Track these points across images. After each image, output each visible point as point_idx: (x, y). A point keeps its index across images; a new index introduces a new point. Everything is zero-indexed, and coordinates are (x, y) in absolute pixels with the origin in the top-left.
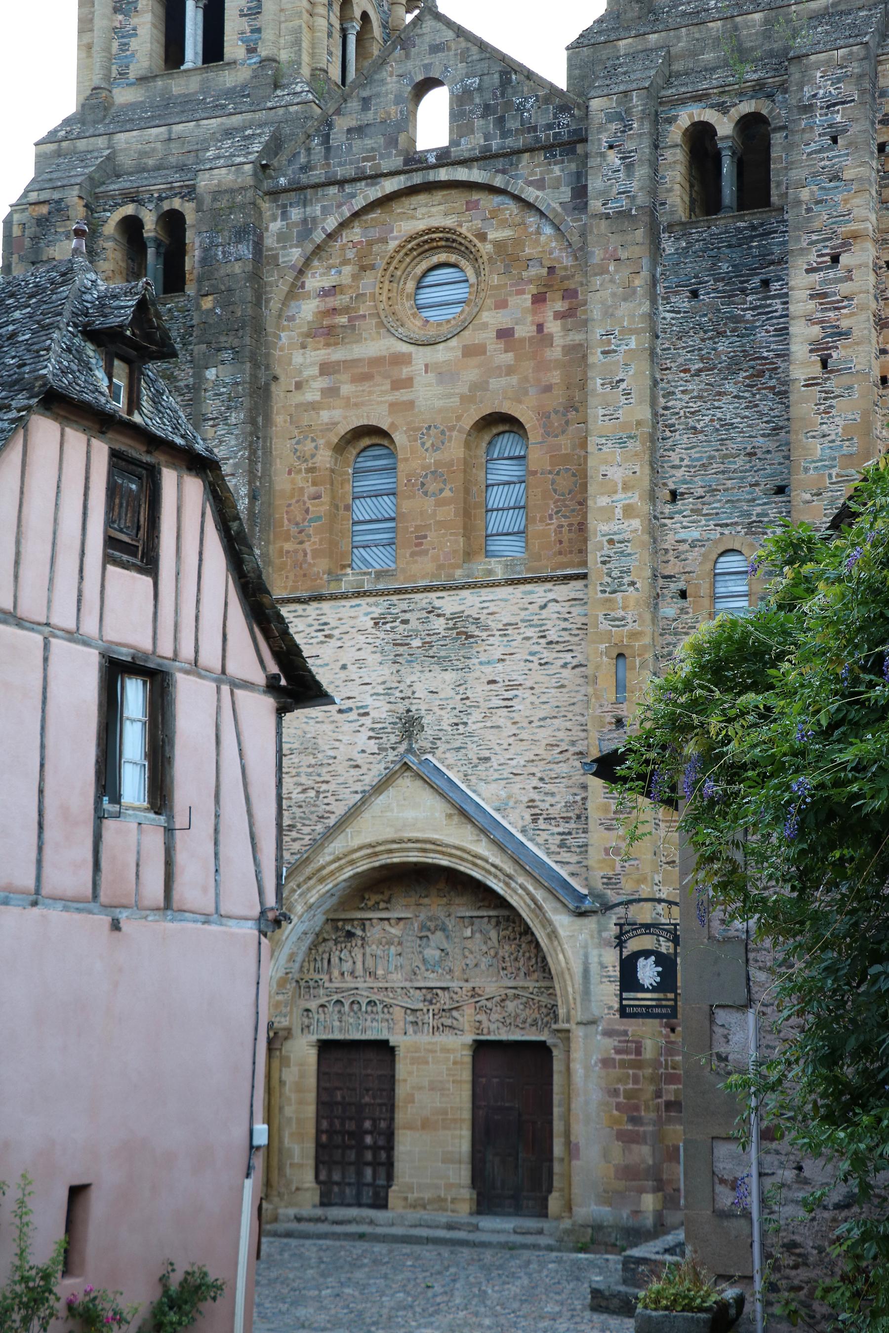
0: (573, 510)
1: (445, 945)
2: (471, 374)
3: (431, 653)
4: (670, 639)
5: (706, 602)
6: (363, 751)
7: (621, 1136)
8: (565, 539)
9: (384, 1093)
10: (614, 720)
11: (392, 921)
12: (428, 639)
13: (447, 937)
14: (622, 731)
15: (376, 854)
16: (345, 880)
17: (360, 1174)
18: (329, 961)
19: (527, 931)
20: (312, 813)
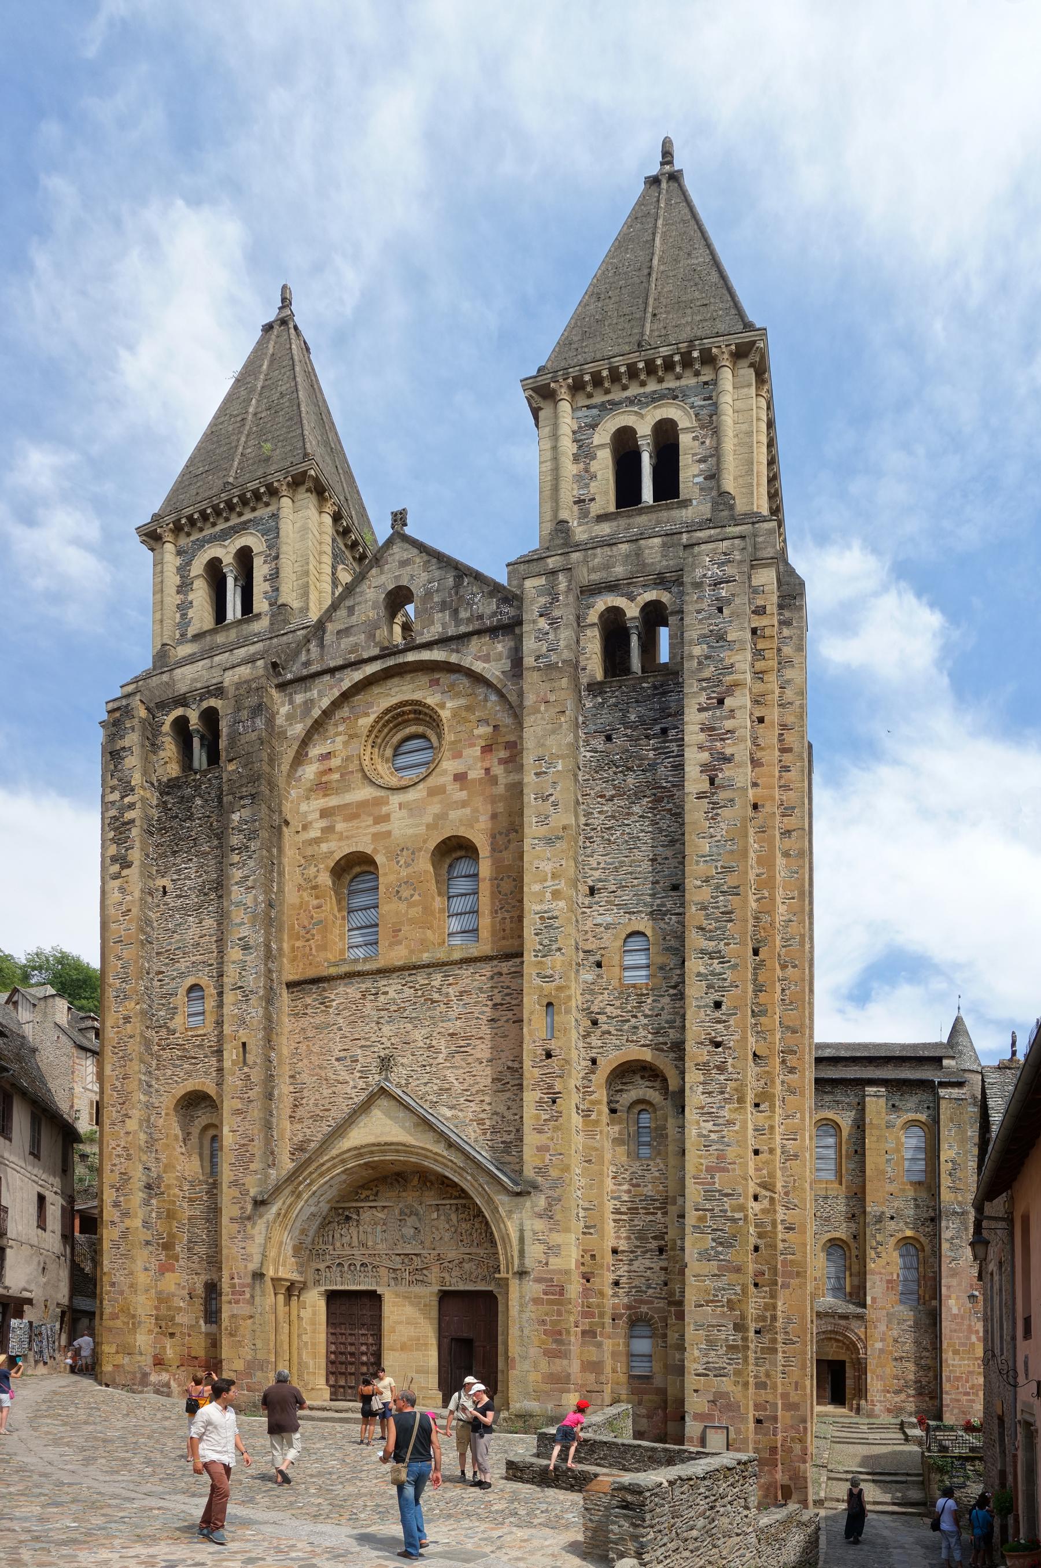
0: (514, 907)
2: (435, 808)
4: (588, 997)
5: (617, 969)
8: (508, 928)
12: (403, 1005)
19: (480, 1213)
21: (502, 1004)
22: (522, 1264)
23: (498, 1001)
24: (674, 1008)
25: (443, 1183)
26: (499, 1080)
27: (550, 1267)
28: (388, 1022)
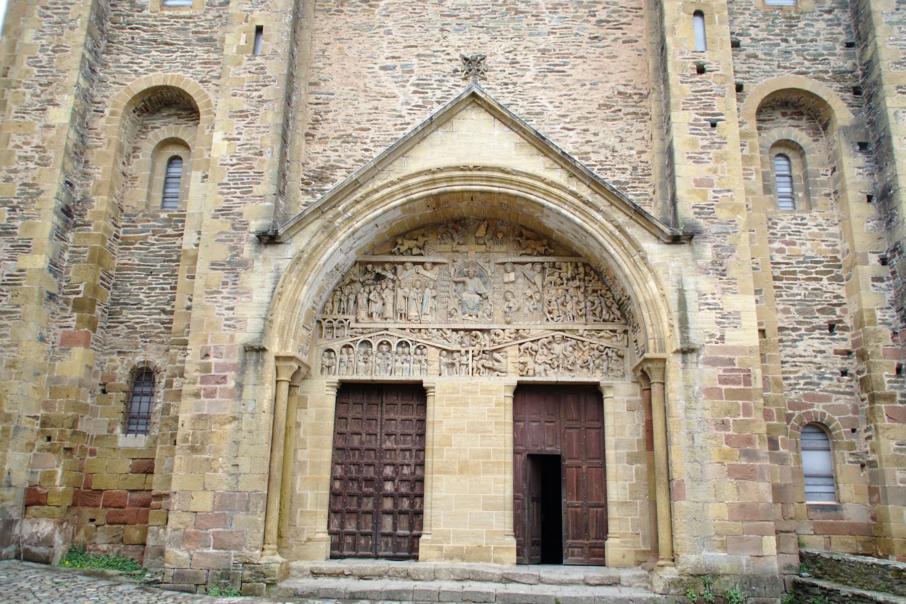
1: (483, 290)
3: (480, 24)
6: (407, 103)
7: (733, 472)
9: (409, 438)
10: (695, 66)
11: (428, 266)
12: (477, 13)
13: (485, 283)
14: (703, 75)
15: (434, 181)
16: (395, 208)
17: (377, 524)
18: (356, 302)
20: (348, 157)
21: (608, 22)
22: (685, 339)
23: (603, 17)
24: (832, 34)
25: (521, 235)
26: (609, 107)
27: (728, 343)
28: (457, 30)
